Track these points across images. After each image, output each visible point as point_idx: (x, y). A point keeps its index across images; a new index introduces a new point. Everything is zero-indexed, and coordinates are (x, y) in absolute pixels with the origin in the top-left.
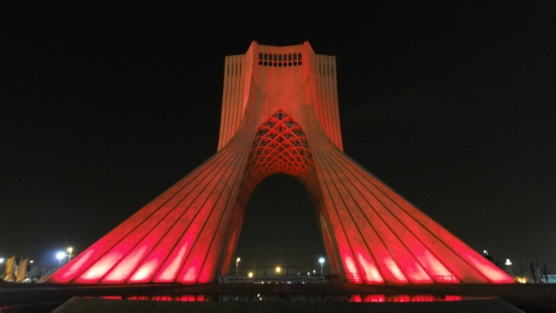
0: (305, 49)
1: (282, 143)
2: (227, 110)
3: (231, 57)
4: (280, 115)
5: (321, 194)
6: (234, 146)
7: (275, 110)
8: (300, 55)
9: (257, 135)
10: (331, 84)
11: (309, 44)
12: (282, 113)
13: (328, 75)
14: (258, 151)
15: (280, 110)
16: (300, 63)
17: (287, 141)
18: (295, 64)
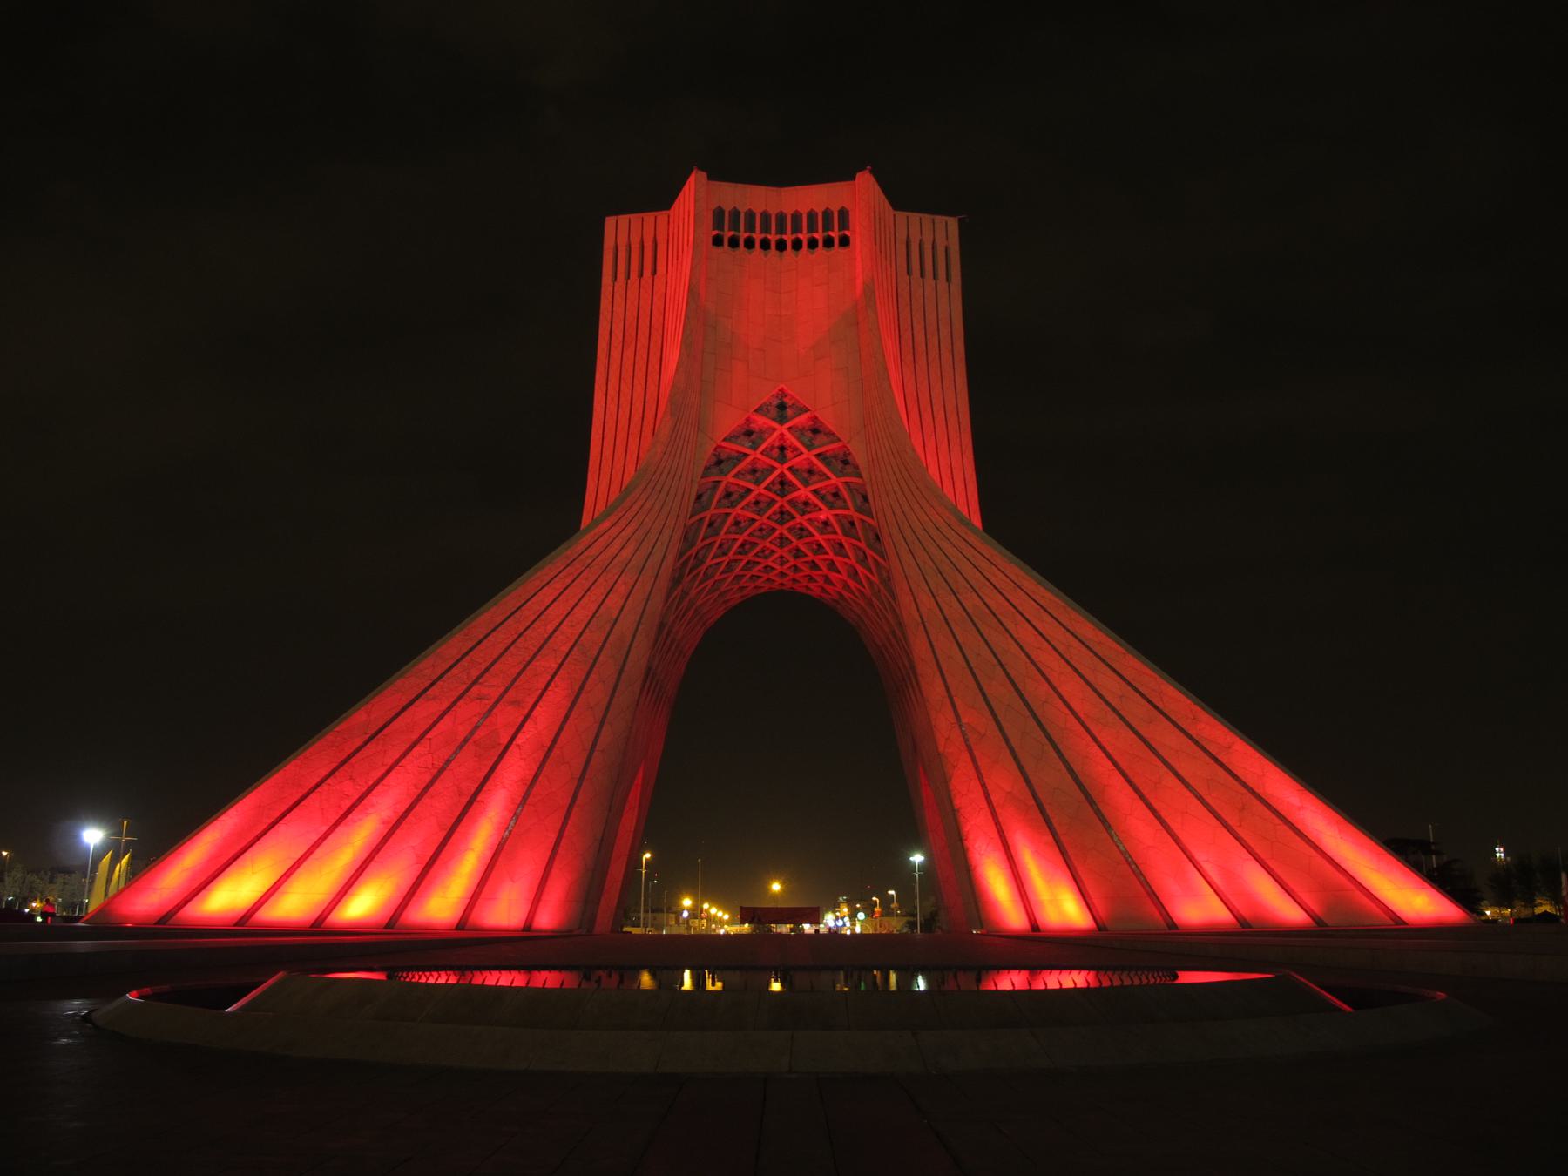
0: (861, 195)
1: (790, 497)
2: (613, 393)
3: (623, 220)
4: (782, 407)
5: (911, 661)
6: (636, 507)
7: (765, 393)
8: (843, 214)
9: (706, 468)
10: (943, 305)
11: (873, 180)
12: (789, 402)
13: (935, 277)
14: (711, 524)
15: (782, 392)
16: (845, 242)
17: (804, 493)
18: (828, 243)
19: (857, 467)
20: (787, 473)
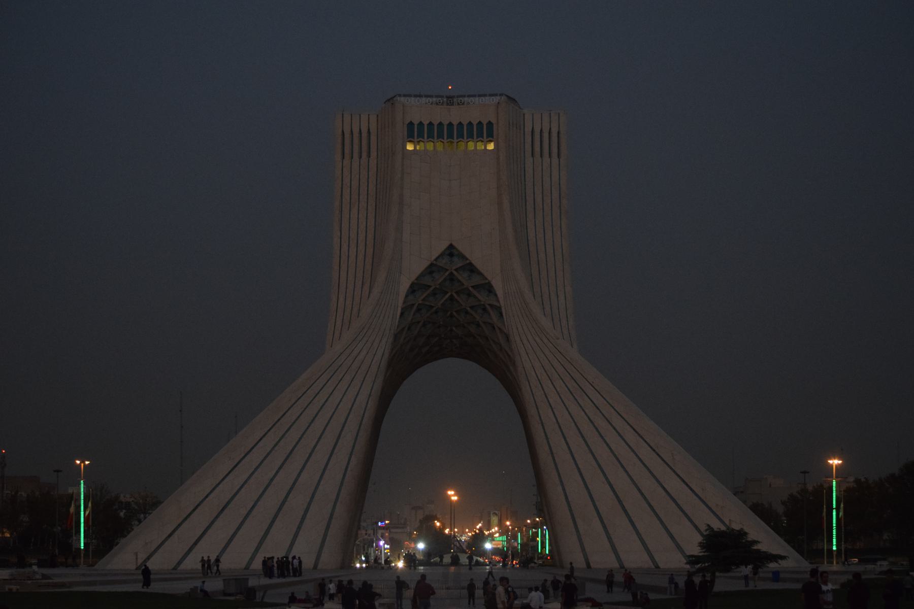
9: (407, 296)
13: (550, 156)
15: (451, 246)
19: (496, 295)
20: (455, 295)
